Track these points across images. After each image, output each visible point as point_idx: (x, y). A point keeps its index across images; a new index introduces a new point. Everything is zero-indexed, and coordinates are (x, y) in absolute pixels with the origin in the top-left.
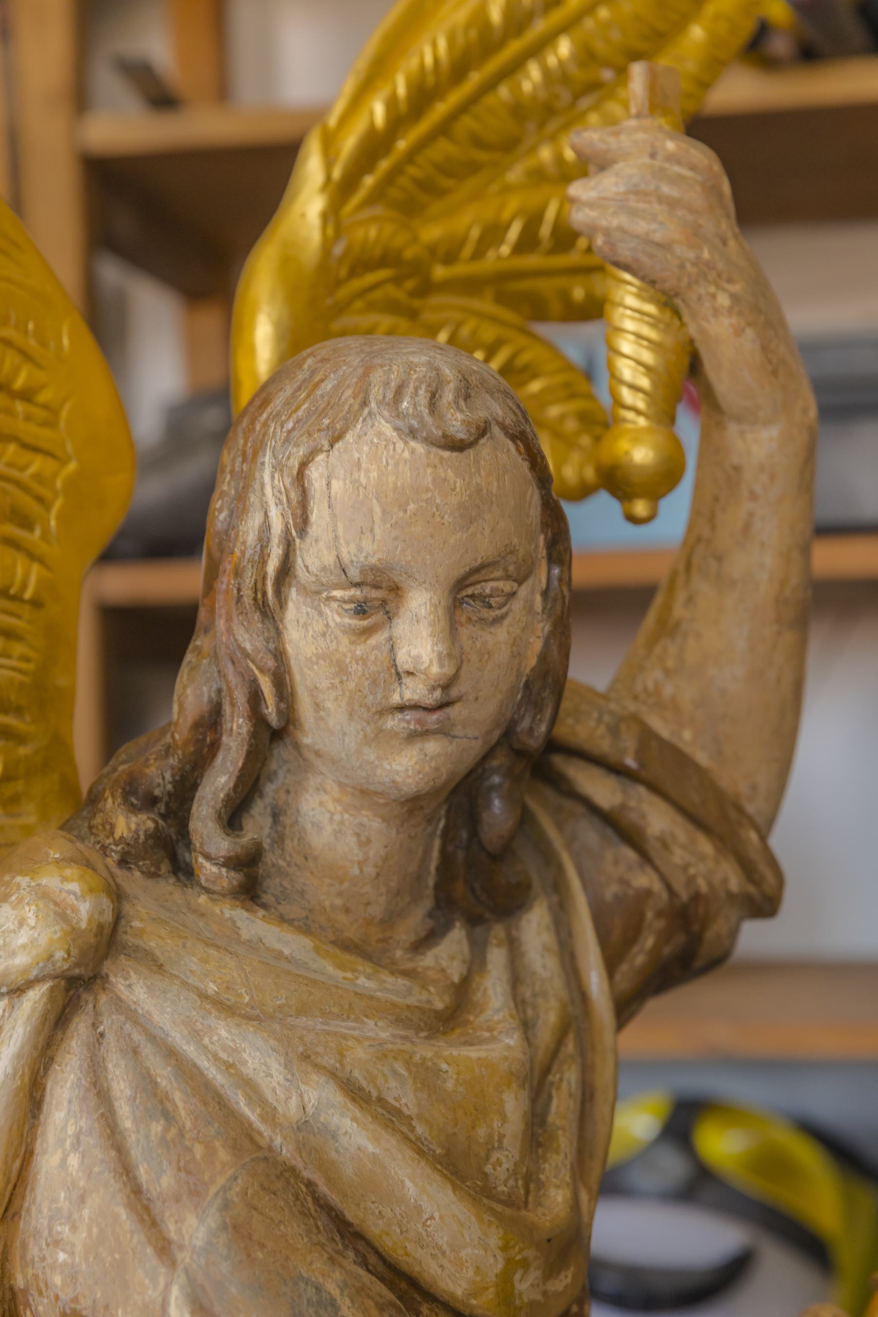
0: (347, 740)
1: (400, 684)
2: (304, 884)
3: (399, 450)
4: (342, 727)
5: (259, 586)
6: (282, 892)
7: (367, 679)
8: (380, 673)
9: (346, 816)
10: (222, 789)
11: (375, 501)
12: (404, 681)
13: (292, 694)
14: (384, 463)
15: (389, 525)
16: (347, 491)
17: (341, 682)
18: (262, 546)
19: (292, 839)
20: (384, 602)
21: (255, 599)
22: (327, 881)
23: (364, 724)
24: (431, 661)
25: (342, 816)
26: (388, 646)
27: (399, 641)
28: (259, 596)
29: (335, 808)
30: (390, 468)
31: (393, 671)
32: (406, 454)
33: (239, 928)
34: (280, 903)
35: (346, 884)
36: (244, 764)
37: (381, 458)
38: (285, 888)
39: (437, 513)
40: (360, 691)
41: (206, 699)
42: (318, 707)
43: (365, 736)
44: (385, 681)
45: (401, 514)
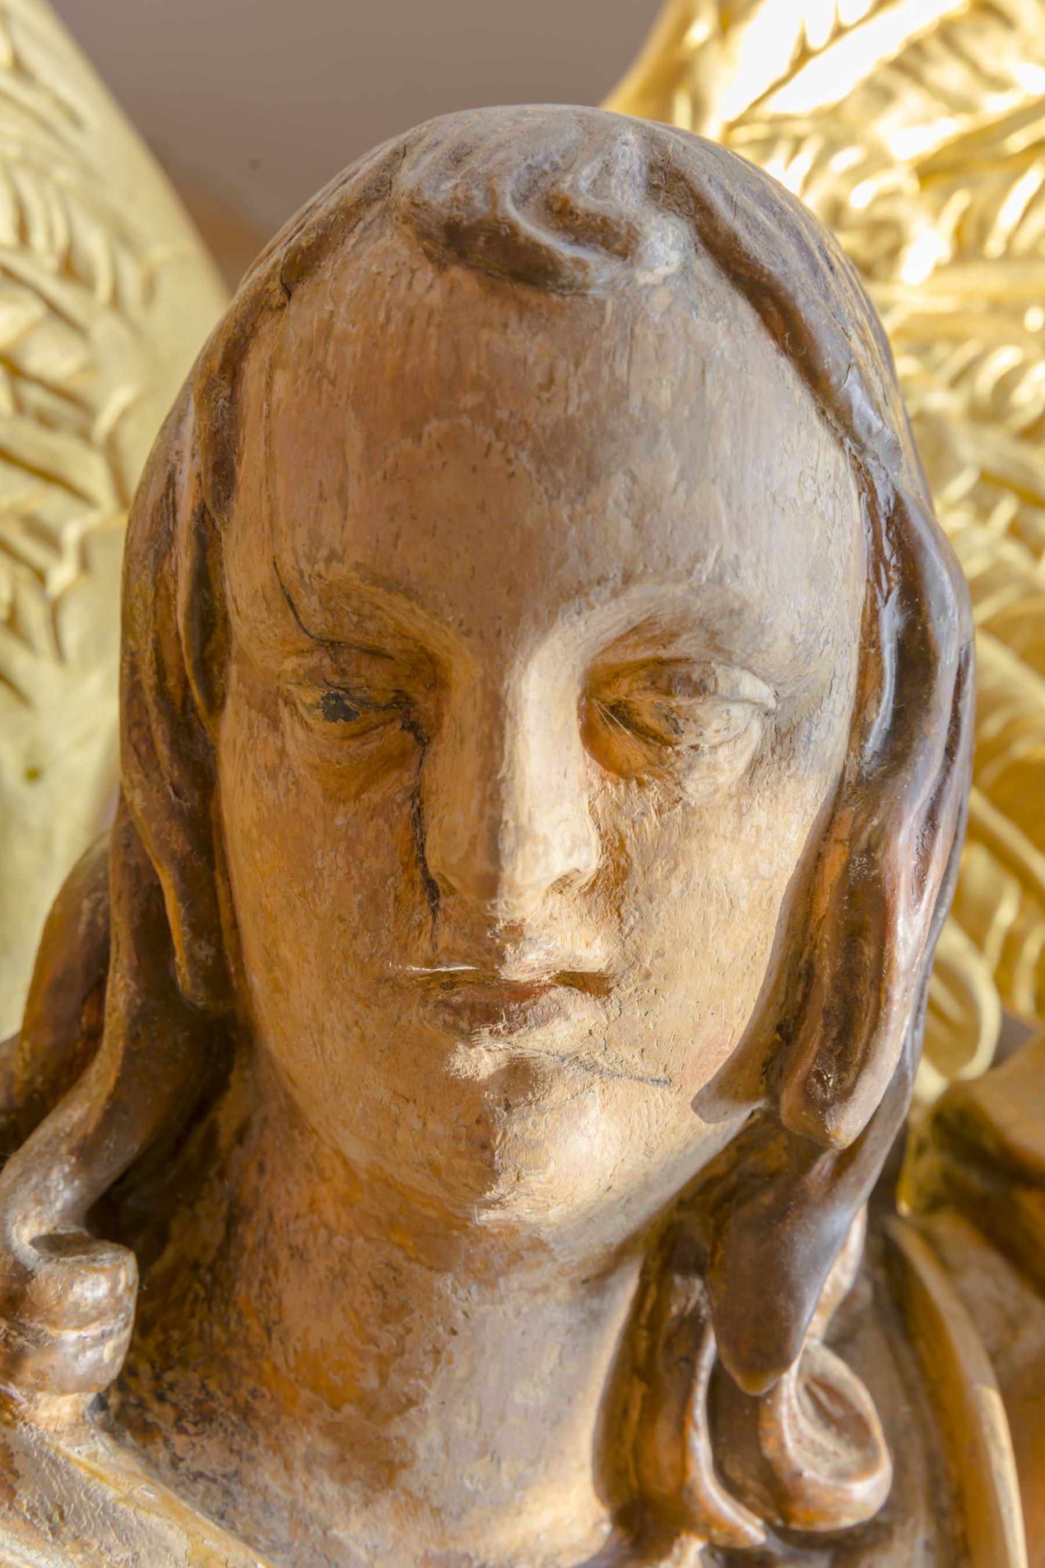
0: (327, 1042)
1: (434, 911)
2: (253, 1393)
3: (419, 288)
4: (314, 1010)
5: (170, 660)
6: (198, 1402)
7: (356, 890)
8: (385, 878)
9: (360, 1241)
10: (69, 1135)
11: (351, 414)
12: (442, 902)
13: (235, 925)
14: (382, 317)
15: (379, 474)
16: (296, 393)
17: (303, 894)
18: (157, 552)
19: (249, 1283)
20: (402, 702)
21: (161, 690)
22: (306, 1394)
23: (358, 1007)
24: (473, 842)
25: (351, 1240)
26: (408, 810)
27: (433, 798)
28: (171, 683)
29: (339, 1218)
30: (392, 328)
31: (418, 875)
32: (435, 297)
33: (15, 1473)
34: (182, 1431)
35: (348, 1409)
36: (119, 1082)
37: (377, 308)
38: (210, 1396)
39: (499, 446)
40: (342, 920)
41: (82, 928)
42: (272, 961)
43: (362, 1037)
44: (396, 898)
45: (408, 445)
